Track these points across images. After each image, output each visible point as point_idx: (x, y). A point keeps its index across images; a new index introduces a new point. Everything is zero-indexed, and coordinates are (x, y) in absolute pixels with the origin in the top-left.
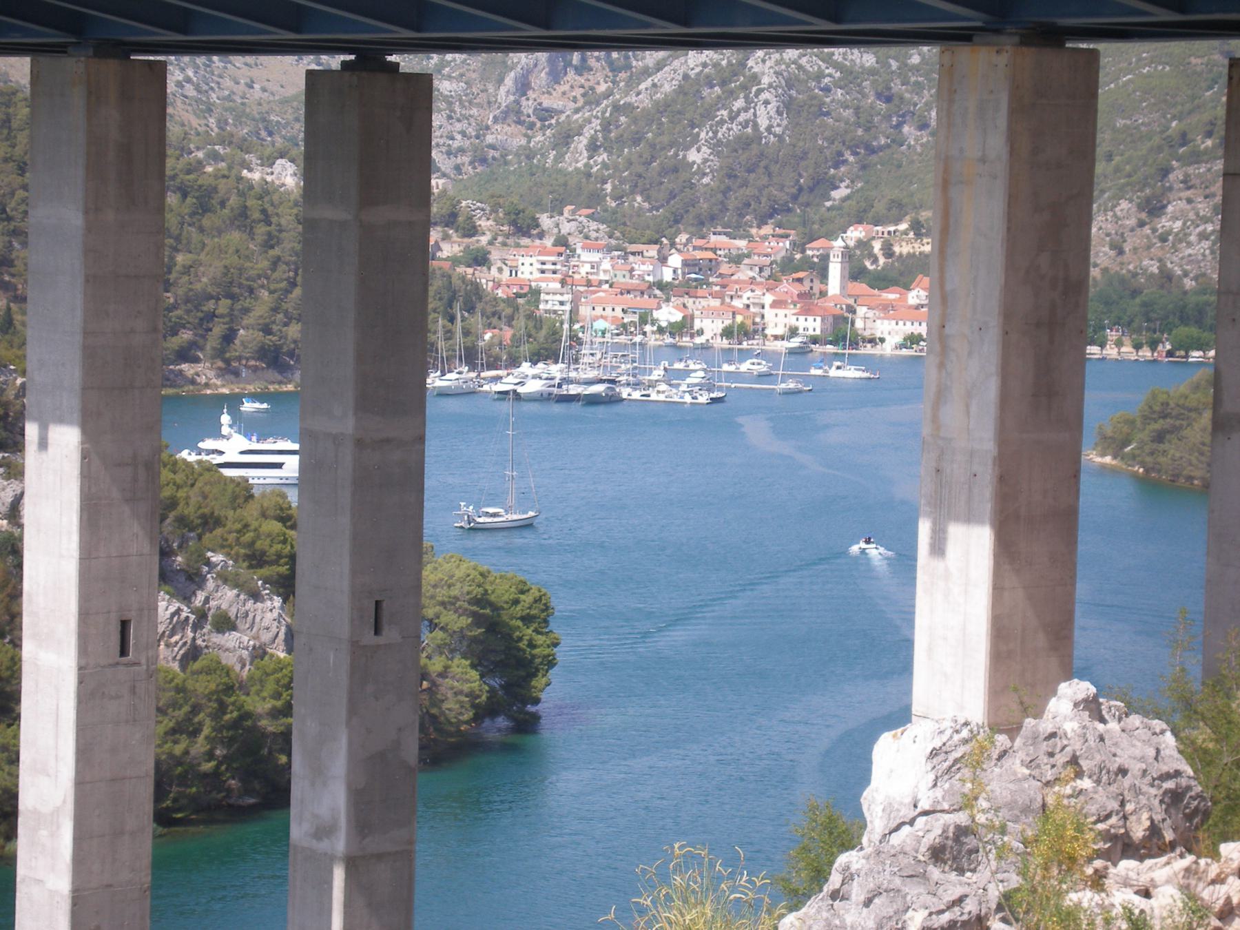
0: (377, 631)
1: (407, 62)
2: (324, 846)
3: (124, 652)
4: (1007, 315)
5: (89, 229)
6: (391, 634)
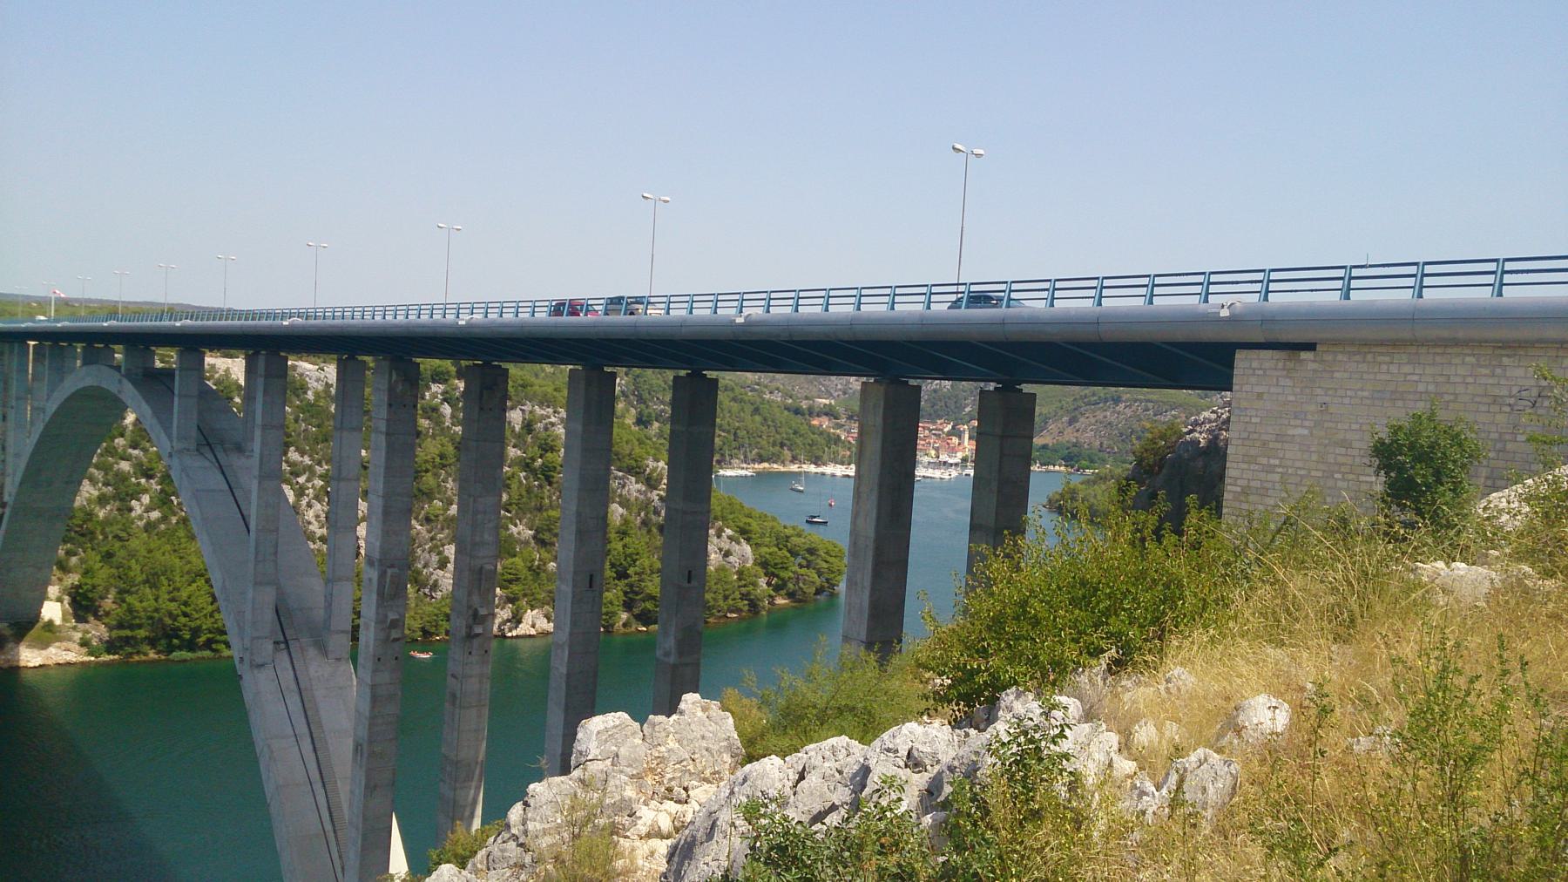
0: (689, 582)
3: (591, 587)
4: (881, 486)
6: (694, 583)
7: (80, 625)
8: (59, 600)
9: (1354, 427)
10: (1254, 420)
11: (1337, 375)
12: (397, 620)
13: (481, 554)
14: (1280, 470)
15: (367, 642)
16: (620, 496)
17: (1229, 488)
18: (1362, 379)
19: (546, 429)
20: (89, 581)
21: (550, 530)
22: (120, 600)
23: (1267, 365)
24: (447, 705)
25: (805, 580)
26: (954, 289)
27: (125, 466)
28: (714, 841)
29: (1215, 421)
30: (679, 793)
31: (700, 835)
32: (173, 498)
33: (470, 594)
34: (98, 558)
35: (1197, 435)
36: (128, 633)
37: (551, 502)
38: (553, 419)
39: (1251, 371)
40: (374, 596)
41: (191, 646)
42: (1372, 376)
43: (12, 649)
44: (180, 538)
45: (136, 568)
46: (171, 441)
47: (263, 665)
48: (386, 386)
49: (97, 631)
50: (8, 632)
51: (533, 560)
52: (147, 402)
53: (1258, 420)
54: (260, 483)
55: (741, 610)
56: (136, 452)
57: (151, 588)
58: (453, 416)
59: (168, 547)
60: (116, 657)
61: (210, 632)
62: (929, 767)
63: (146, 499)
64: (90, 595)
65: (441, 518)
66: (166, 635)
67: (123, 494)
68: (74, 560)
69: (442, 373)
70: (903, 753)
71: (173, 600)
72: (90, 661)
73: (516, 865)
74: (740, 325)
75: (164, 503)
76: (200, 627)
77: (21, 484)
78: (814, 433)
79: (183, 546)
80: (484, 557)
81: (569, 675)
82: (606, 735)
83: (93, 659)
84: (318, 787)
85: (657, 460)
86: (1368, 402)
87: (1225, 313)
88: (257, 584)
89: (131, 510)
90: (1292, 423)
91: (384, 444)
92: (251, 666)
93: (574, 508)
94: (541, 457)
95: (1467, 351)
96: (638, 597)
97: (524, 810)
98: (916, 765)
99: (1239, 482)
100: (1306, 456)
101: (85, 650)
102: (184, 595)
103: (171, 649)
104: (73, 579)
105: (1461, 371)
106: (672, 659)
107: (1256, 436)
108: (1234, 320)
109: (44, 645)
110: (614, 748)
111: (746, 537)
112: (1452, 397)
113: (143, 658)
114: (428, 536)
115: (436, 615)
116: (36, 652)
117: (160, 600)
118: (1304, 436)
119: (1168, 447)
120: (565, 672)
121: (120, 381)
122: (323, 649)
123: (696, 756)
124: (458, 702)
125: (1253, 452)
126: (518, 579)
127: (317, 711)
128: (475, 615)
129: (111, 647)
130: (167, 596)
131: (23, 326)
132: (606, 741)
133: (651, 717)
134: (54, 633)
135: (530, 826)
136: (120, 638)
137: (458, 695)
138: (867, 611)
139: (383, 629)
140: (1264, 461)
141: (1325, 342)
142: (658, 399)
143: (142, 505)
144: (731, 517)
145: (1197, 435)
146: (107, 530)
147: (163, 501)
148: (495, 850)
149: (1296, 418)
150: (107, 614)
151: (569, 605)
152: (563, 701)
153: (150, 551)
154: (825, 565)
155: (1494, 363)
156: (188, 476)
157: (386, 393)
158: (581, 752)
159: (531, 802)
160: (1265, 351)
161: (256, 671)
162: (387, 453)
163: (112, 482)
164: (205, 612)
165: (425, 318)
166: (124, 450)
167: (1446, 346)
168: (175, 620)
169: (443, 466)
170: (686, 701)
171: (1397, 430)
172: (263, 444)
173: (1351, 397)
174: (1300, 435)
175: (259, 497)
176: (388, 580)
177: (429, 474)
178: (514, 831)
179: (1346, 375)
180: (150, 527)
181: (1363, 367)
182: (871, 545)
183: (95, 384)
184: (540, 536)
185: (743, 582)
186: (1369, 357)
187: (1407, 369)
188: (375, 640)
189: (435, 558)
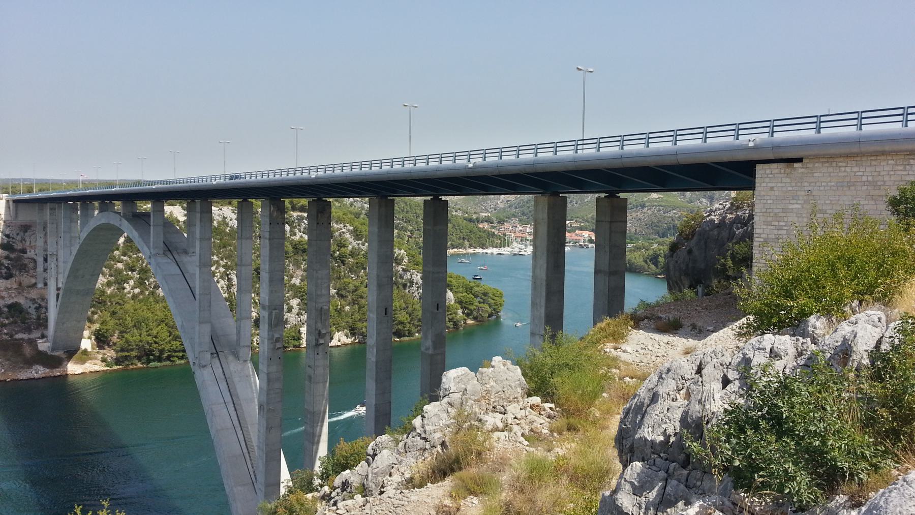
4: (548, 251)
5: (379, 232)
6: (440, 310)
7: (101, 351)
8: (90, 338)
9: (827, 202)
10: (769, 202)
11: (815, 175)
12: (279, 338)
14: (785, 228)
17: (756, 239)
18: (830, 176)
19: (340, 235)
21: (345, 289)
22: (121, 337)
23: (775, 171)
24: (307, 382)
27: (120, 265)
28: (659, 403)
29: (722, 209)
30: (500, 409)
31: (647, 401)
32: (146, 281)
34: (109, 315)
35: (713, 217)
37: (345, 274)
38: (344, 230)
39: (766, 176)
40: (267, 326)
41: (159, 359)
42: (836, 174)
45: (129, 319)
47: (205, 366)
48: (268, 213)
49: (110, 354)
50: (64, 356)
51: (338, 306)
52: (136, 230)
53: (771, 201)
54: (200, 269)
56: (125, 258)
58: (291, 231)
60: (121, 367)
61: (169, 351)
62: (783, 357)
63: (132, 282)
64: (106, 335)
65: (287, 285)
66: (147, 355)
67: (120, 281)
68: (96, 316)
70: (768, 350)
71: (149, 335)
72: (107, 370)
73: (421, 449)
74: (471, 168)
76: (164, 348)
77: (68, 277)
78: (480, 232)
80: (323, 302)
81: (377, 362)
82: (458, 379)
83: (108, 368)
85: (400, 249)
86: (835, 188)
87: (751, 144)
88: (200, 323)
89: (124, 288)
90: (791, 202)
93: (376, 273)
94: (338, 251)
95: (889, 158)
97: (422, 420)
98: (776, 356)
99: (762, 236)
100: (800, 219)
101: (104, 364)
102: (154, 332)
103: (149, 361)
104: (96, 326)
105: (886, 168)
106: (430, 352)
107: (771, 210)
108: (756, 148)
109: (83, 362)
110: (463, 386)
112: (882, 183)
113: (135, 367)
115: (288, 337)
116: (79, 366)
118: (799, 209)
119: (697, 225)
120: (375, 360)
121: (120, 220)
122: (236, 355)
123: (505, 389)
125: (769, 219)
128: (320, 333)
129: (118, 361)
130: (145, 333)
132: (459, 382)
133: (480, 369)
135: (427, 428)
136: (122, 357)
137: (313, 377)
139: (272, 343)
140: (776, 223)
141: (808, 157)
145: (713, 217)
146: (112, 300)
147: (141, 283)
148: (409, 441)
149: (793, 199)
150: (115, 344)
151: (375, 324)
153: (136, 310)
154: (493, 301)
155: (904, 163)
156: (160, 267)
158: (446, 389)
159: (426, 415)
160: (773, 164)
161: (202, 369)
165: (291, 176)
166: (119, 258)
167: (877, 156)
170: (495, 361)
171: (903, 191)
172: (201, 248)
173: (824, 186)
174: (796, 209)
175: (200, 277)
178: (418, 431)
179: (822, 175)
180: (134, 297)
181: (831, 170)
182: (544, 283)
184: (340, 292)
186: (834, 164)
187: (856, 169)
188: (268, 349)
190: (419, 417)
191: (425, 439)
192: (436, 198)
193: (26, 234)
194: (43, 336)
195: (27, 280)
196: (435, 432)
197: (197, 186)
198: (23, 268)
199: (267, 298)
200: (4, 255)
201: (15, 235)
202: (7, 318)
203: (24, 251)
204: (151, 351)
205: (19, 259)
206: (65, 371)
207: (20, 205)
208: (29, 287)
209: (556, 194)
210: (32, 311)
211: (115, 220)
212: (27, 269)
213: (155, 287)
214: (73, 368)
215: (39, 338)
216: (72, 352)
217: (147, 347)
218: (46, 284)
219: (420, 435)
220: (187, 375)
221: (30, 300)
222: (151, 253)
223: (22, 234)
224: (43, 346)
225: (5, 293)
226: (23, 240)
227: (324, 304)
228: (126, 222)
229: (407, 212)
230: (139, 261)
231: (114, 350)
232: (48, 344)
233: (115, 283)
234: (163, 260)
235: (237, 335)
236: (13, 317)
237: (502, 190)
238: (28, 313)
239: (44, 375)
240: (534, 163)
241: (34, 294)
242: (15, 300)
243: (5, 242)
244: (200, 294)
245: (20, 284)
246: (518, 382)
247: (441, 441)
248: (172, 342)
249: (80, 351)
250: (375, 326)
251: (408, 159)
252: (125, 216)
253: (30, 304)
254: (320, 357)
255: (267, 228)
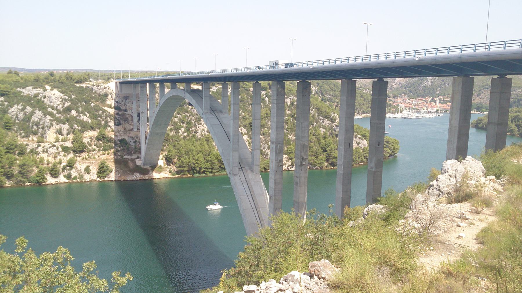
1: (385, 79)
2: (372, 170)
4: (461, 110)
7: (168, 167)
8: (162, 159)
12: (281, 160)
13: (304, 140)
15: (272, 166)
16: (323, 125)
20: (170, 154)
22: (179, 159)
24: (295, 186)
25: (385, 152)
26: (485, 45)
27: (176, 120)
32: (190, 129)
33: (301, 152)
34: (172, 147)
36: (182, 169)
41: (199, 172)
43: (151, 173)
44: (194, 141)
45: (183, 150)
46: (203, 110)
47: (236, 175)
48: (276, 89)
49: (174, 168)
50: (150, 169)
52: (194, 99)
54: (233, 121)
55: (364, 162)
56: (179, 116)
57: (187, 155)
58: (269, 101)
59: (190, 144)
60: (179, 176)
61: (204, 168)
63: (183, 129)
64: (171, 158)
65: (267, 133)
66: (192, 170)
67: (177, 129)
68: (165, 148)
69: (265, 88)
71: (193, 159)
72: (172, 177)
74: (417, 60)
75: (188, 131)
76: (202, 167)
77: (153, 125)
79: (195, 143)
80: (305, 141)
81: (343, 174)
83: (173, 176)
84: (255, 210)
85: (334, 113)
88: (233, 151)
89: (179, 133)
91: (276, 107)
92: (233, 175)
96: (331, 158)
101: (170, 174)
102: (196, 157)
103: (194, 173)
104: (166, 153)
106: (374, 170)
109: (160, 172)
111: (365, 137)
113: (186, 176)
114: (264, 139)
117: (190, 159)
120: (342, 173)
121: (185, 93)
122: (252, 170)
123: (475, 171)
124: (298, 185)
126: (292, 152)
127: (252, 188)
128: (303, 158)
129: (178, 173)
130: (192, 158)
131: (145, 79)
134: (162, 169)
135: (441, 186)
136: (180, 170)
137: (298, 183)
138: (456, 150)
142: (328, 94)
143: (182, 131)
144: (359, 131)
146: (173, 139)
147: (187, 130)
150: (176, 163)
152: (342, 182)
153: (186, 145)
154: (392, 147)
156: (208, 120)
157: (276, 91)
158: (446, 169)
159: (439, 180)
161: (234, 176)
162: (277, 109)
163: (173, 125)
164: (203, 162)
166: (176, 115)
168: (194, 165)
169: (267, 117)
172: (234, 109)
175: (233, 125)
176: (278, 148)
177: (263, 120)
178: (435, 187)
180: (184, 138)
183: (176, 94)
185: (365, 153)
189: (266, 146)
190: (435, 181)
191: (439, 190)
192: (380, 80)
193: (127, 101)
194: (138, 158)
195: (128, 127)
196: (444, 188)
197: (217, 75)
198: (126, 120)
199: (275, 137)
200: (116, 112)
201: (121, 101)
202: (120, 147)
203: (126, 111)
204: (195, 168)
205: (123, 115)
206: (150, 177)
207: (123, 85)
208: (129, 130)
209: (467, 76)
210: (132, 143)
211: (181, 94)
212: (128, 121)
213: (195, 132)
214: (156, 175)
215: (136, 158)
216: (154, 167)
217: (193, 165)
218: (138, 129)
219: (436, 188)
220: (226, 181)
221: (131, 138)
222: (203, 112)
223: (124, 101)
224: (139, 163)
225: (117, 133)
226: (125, 104)
227: (305, 142)
228: (188, 94)
229: (335, 90)
230: (186, 118)
231: (175, 166)
232: (141, 162)
233: (174, 129)
234: (210, 116)
235: (252, 158)
236: (122, 147)
237: (453, 73)
238: (130, 145)
239: (140, 179)
240: (460, 57)
241: (132, 134)
242: (123, 137)
243: (116, 105)
244: (233, 135)
245: (125, 129)
246: (481, 169)
247: (447, 192)
248: (206, 164)
249: (158, 166)
250: (343, 154)
251: (365, 57)
252: (187, 91)
253: (130, 140)
254: (303, 172)
255: (275, 97)
